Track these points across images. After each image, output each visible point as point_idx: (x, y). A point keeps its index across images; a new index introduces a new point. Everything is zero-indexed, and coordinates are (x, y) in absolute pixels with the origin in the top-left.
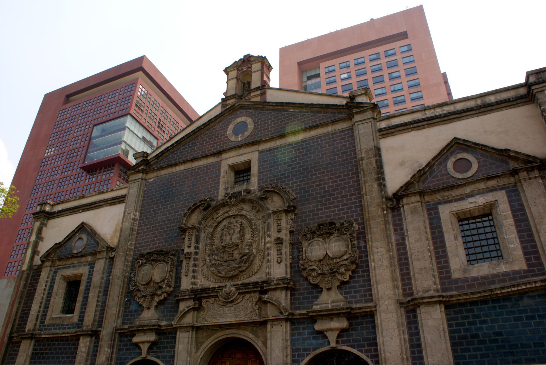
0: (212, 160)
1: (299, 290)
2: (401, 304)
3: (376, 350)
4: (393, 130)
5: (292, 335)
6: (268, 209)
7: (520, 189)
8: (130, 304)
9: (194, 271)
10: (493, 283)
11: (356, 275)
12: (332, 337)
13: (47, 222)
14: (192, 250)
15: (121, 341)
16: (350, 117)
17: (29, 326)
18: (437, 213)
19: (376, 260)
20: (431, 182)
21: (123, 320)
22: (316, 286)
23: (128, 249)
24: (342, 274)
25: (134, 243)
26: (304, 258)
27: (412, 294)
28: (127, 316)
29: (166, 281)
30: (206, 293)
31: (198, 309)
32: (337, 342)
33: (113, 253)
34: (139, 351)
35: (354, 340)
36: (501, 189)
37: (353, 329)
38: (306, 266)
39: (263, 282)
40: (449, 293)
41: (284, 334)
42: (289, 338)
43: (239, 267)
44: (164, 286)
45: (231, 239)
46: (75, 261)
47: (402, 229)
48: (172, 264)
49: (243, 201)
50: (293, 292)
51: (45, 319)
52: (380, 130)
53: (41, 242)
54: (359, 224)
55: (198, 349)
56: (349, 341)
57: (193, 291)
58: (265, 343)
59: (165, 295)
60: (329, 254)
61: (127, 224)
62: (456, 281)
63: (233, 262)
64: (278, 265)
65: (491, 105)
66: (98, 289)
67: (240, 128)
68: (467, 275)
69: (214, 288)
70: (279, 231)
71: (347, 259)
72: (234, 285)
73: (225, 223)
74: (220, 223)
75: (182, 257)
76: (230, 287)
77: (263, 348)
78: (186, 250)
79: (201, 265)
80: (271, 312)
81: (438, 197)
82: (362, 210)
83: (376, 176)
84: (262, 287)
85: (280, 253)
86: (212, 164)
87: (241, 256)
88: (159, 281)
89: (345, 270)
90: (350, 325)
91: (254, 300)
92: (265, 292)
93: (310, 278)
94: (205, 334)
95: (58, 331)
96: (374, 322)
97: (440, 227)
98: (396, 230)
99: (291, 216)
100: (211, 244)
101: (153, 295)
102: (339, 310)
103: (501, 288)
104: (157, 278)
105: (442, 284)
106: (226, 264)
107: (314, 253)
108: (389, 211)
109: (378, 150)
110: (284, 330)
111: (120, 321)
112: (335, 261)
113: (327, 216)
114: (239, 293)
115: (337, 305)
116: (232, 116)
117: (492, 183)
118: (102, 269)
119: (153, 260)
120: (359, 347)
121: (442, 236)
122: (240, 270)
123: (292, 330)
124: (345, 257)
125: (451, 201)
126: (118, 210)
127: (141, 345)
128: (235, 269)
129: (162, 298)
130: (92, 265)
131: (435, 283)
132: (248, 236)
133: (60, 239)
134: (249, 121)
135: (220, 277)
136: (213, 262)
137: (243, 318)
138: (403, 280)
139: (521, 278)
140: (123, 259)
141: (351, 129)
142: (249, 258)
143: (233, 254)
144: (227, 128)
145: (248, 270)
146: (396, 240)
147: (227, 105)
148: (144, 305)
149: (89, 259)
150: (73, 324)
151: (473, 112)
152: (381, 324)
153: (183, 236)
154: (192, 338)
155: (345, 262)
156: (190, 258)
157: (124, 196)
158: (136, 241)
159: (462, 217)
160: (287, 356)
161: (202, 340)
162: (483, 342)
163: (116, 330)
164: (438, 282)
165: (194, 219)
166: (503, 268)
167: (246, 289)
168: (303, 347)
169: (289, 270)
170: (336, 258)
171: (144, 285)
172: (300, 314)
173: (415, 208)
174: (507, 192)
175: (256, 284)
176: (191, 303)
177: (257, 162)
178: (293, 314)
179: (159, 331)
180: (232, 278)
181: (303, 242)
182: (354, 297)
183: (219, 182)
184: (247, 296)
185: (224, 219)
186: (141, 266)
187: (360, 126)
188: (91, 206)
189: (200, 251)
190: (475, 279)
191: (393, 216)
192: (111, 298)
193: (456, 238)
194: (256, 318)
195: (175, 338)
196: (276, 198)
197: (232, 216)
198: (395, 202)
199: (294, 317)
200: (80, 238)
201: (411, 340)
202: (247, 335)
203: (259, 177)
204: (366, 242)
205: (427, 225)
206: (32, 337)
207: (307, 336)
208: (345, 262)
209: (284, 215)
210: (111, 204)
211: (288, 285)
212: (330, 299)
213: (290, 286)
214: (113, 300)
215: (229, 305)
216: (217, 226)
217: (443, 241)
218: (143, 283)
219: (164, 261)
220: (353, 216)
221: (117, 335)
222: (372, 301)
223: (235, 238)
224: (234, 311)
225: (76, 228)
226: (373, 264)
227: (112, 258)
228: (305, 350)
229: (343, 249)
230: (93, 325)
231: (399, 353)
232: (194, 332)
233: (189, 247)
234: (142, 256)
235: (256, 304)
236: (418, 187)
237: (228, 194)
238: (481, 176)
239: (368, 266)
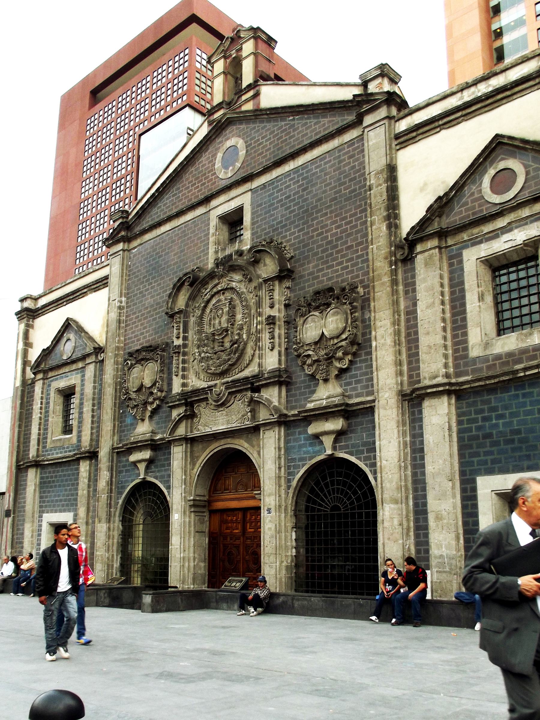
2: (404, 396)
6: (259, 277)
9: (184, 369)
11: (358, 359)
13: (33, 322)
17: (32, 453)
18: (461, 262)
19: (378, 337)
20: (457, 215)
21: (120, 437)
24: (340, 359)
25: (122, 339)
28: (124, 431)
30: (197, 396)
31: (190, 416)
32: (334, 448)
33: (102, 355)
34: (137, 472)
35: (353, 446)
37: (352, 432)
38: (301, 351)
39: (254, 377)
41: (277, 441)
42: (282, 445)
43: (229, 360)
45: (220, 323)
47: (414, 290)
48: (162, 363)
50: (289, 387)
53: (30, 349)
54: (364, 287)
55: (193, 464)
56: (347, 447)
60: (326, 333)
61: (114, 315)
62: (475, 360)
63: (222, 353)
64: (270, 353)
66: (91, 402)
68: (488, 352)
71: (346, 339)
72: (224, 384)
73: (214, 301)
74: (208, 301)
83: (385, 214)
84: (252, 384)
88: (149, 385)
90: (349, 425)
91: (246, 400)
92: (257, 390)
94: (200, 446)
95: (60, 455)
96: (373, 421)
97: (462, 283)
98: (406, 293)
99: (288, 284)
101: (145, 403)
102: (332, 408)
103: (525, 369)
107: (309, 334)
108: (400, 264)
110: (277, 436)
111: (116, 438)
113: (330, 279)
115: (332, 402)
118: (93, 375)
119: (142, 359)
121: (463, 297)
122: (230, 363)
123: (286, 435)
124: (344, 336)
125: (481, 242)
128: (226, 361)
129: (155, 406)
131: (446, 366)
132: (239, 317)
133: (47, 343)
136: (203, 355)
137: (235, 425)
138: (409, 363)
140: (112, 361)
142: (239, 346)
143: (223, 342)
145: (239, 362)
146: (406, 307)
152: (379, 424)
154: (186, 452)
155: (343, 343)
156: (179, 353)
158: (125, 336)
159: (496, 264)
160: (280, 468)
161: (198, 454)
163: (113, 449)
164: (451, 364)
165: (181, 302)
167: (235, 387)
168: (299, 456)
169: (283, 358)
171: (136, 392)
173: (431, 257)
180: (223, 374)
181: (298, 320)
182: (355, 389)
184: (239, 396)
189: (190, 343)
191: (405, 272)
192: (105, 411)
193: (481, 298)
194: (248, 423)
198: (406, 252)
199: (288, 419)
200: (68, 340)
201: (413, 443)
202: (241, 445)
205: (446, 281)
206: (37, 464)
207: (303, 442)
209: (277, 283)
211: (281, 379)
212: (326, 393)
213: (283, 379)
214: (107, 413)
215: (221, 409)
217: (464, 305)
220: (358, 276)
221: (115, 454)
224: (226, 415)
225: (62, 327)
227: (103, 360)
228: (301, 459)
229: (341, 325)
230: (91, 445)
232: (189, 445)
233: (178, 338)
234: (131, 354)
235: (249, 406)
236: (435, 226)
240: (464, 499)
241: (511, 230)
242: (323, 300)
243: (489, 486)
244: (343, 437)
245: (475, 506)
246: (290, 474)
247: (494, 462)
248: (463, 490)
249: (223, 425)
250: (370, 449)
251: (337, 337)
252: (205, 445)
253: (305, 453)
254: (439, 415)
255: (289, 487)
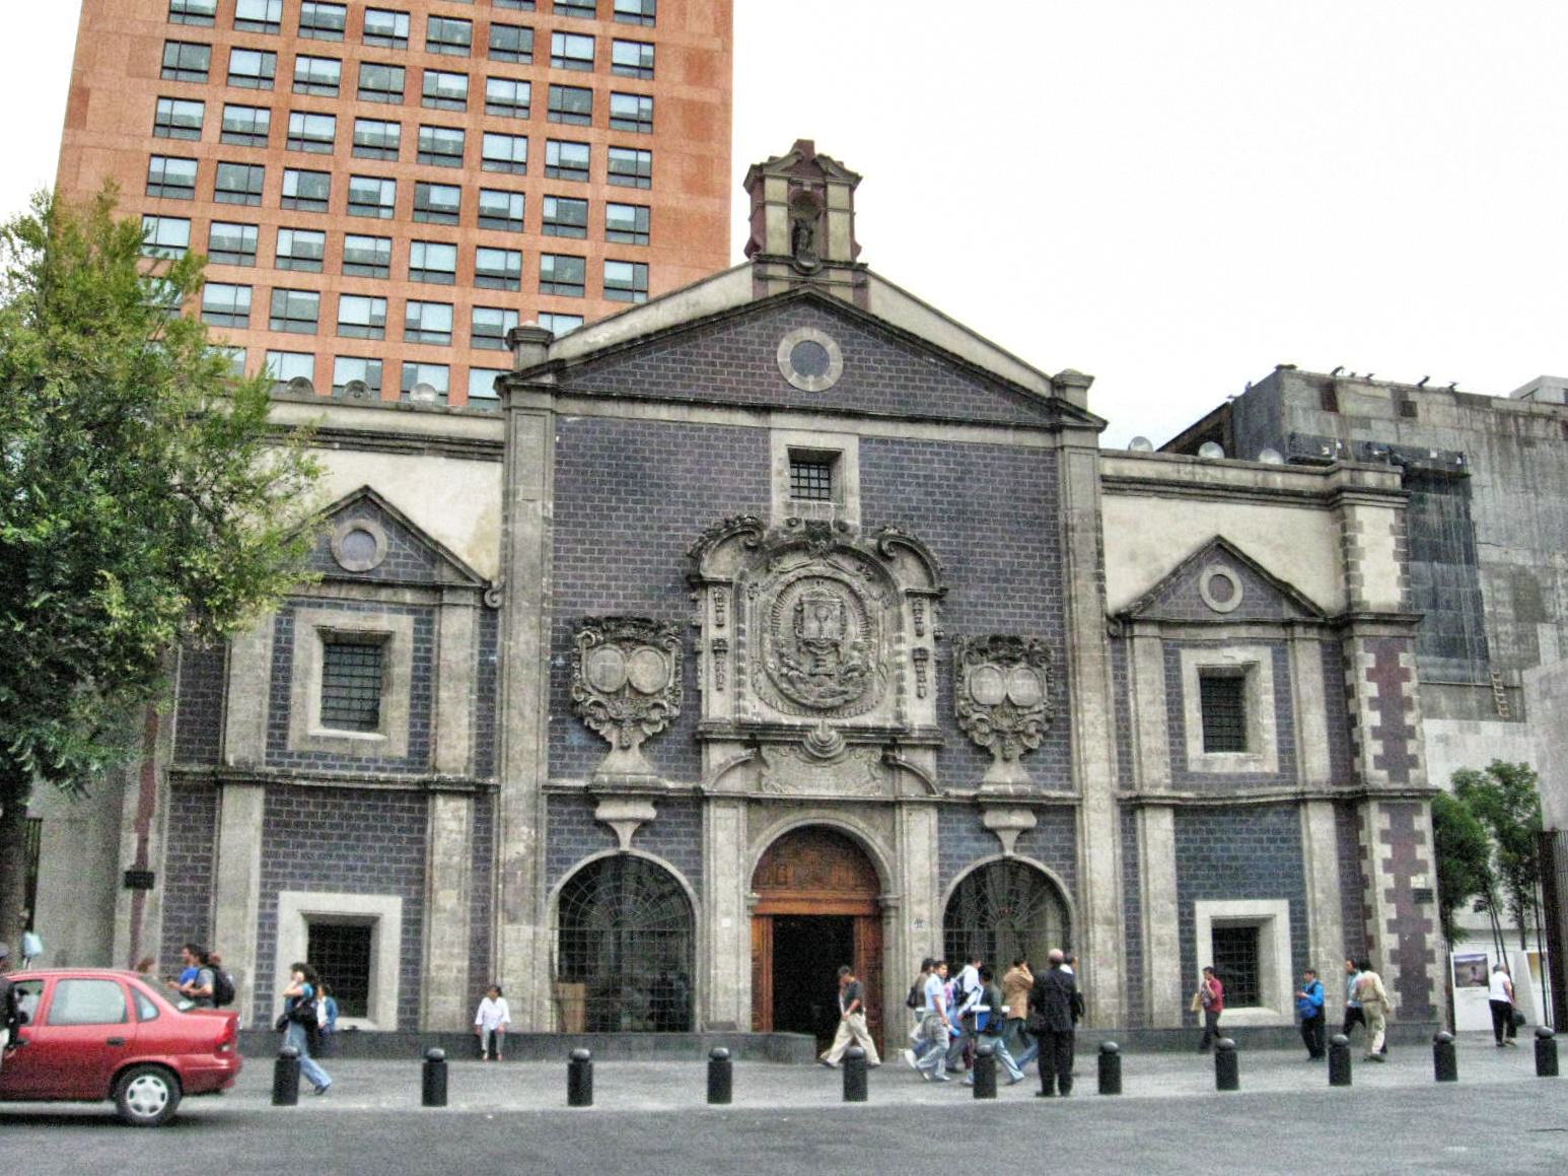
0: (742, 419)
1: (951, 751)
3: (1072, 867)
4: (1125, 486)
5: (940, 830)
7: (1290, 651)
8: (565, 731)
10: (1238, 786)
12: (1009, 839)
14: (726, 633)
15: (549, 812)
16: (1056, 430)
18: (1178, 661)
21: (551, 766)
22: (984, 750)
23: (544, 597)
24: (1030, 736)
26: (967, 695)
27: (1131, 787)
28: (562, 757)
29: (666, 692)
34: (611, 838)
36: (1267, 644)
39: (894, 730)
40: (1184, 794)
44: (666, 704)
45: (821, 630)
46: (356, 593)
47: (1124, 677)
49: (844, 550)
51: (284, 737)
52: (1104, 479)
56: (1031, 849)
57: (742, 726)
58: (891, 841)
59: (666, 723)
60: (1012, 698)
64: (917, 701)
65: (1274, 492)
67: (810, 359)
68: (1206, 770)
69: (791, 727)
70: (920, 634)
72: (836, 727)
73: (800, 590)
74: (790, 585)
75: (704, 644)
76: (824, 728)
77: (886, 849)
78: (712, 633)
79: (749, 671)
80: (910, 789)
81: (1182, 634)
82: (1062, 626)
83: (1093, 570)
84: (894, 740)
85: (921, 677)
86: (746, 429)
87: (843, 669)
89: (1037, 731)
93: (970, 734)
94: (764, 813)
96: (1073, 822)
98: (1116, 677)
100: (774, 631)
101: (638, 722)
104: (646, 683)
105: (1174, 777)
106: (816, 680)
107: (985, 692)
109: (1098, 515)
111: (545, 768)
112: (1020, 711)
114: (849, 745)
116: (784, 316)
117: (1256, 631)
119: (628, 639)
120: (1047, 860)
122: (846, 697)
123: (940, 821)
124: (1036, 709)
126: (485, 477)
127: (615, 826)
128: (833, 694)
129: (660, 728)
130: (425, 619)
134: (831, 346)
135: (804, 705)
136: (785, 670)
137: (852, 792)
138: (1120, 762)
139: (1271, 785)
140: (534, 619)
141: (1053, 452)
144: (777, 344)
146: (1116, 694)
147: (772, 278)
148: (613, 738)
149: (408, 597)
150: (389, 760)
151: (1249, 496)
153: (693, 595)
157: (498, 446)
162: (1215, 867)
166: (1252, 768)
170: (1023, 707)
171: (608, 694)
172: (957, 797)
174: (1274, 652)
175: (879, 731)
176: (744, 753)
177: (856, 461)
178: (947, 795)
179: (661, 801)
183: (768, 482)
184: (860, 751)
185: (799, 579)
186: (592, 647)
187: (1073, 457)
188: (377, 442)
190: (1217, 776)
191: (1114, 651)
195: (699, 816)
196: (911, 563)
197: (814, 577)
202: (853, 823)
203: (862, 498)
204: (1066, 685)
208: (1037, 717)
210: (451, 454)
212: (1004, 777)
214: (522, 715)
216: (782, 593)
217: (1181, 711)
218: (606, 689)
219: (655, 644)
222: (1070, 788)
223: (830, 628)
226: (1081, 729)
228: (960, 857)
231: (1110, 874)
236: (1157, 612)
237: (798, 521)
238: (1244, 617)
239: (1068, 728)
240: (1181, 923)
241: (1229, 646)
242: (1005, 649)
243: (1207, 911)
244: (1026, 836)
245: (1193, 932)
246: (944, 875)
247: (1213, 887)
248: (1181, 914)
249: (828, 788)
250: (1069, 856)
251: (1030, 707)
252: (773, 813)
253: (967, 849)
254: (1159, 830)
255: (942, 893)
